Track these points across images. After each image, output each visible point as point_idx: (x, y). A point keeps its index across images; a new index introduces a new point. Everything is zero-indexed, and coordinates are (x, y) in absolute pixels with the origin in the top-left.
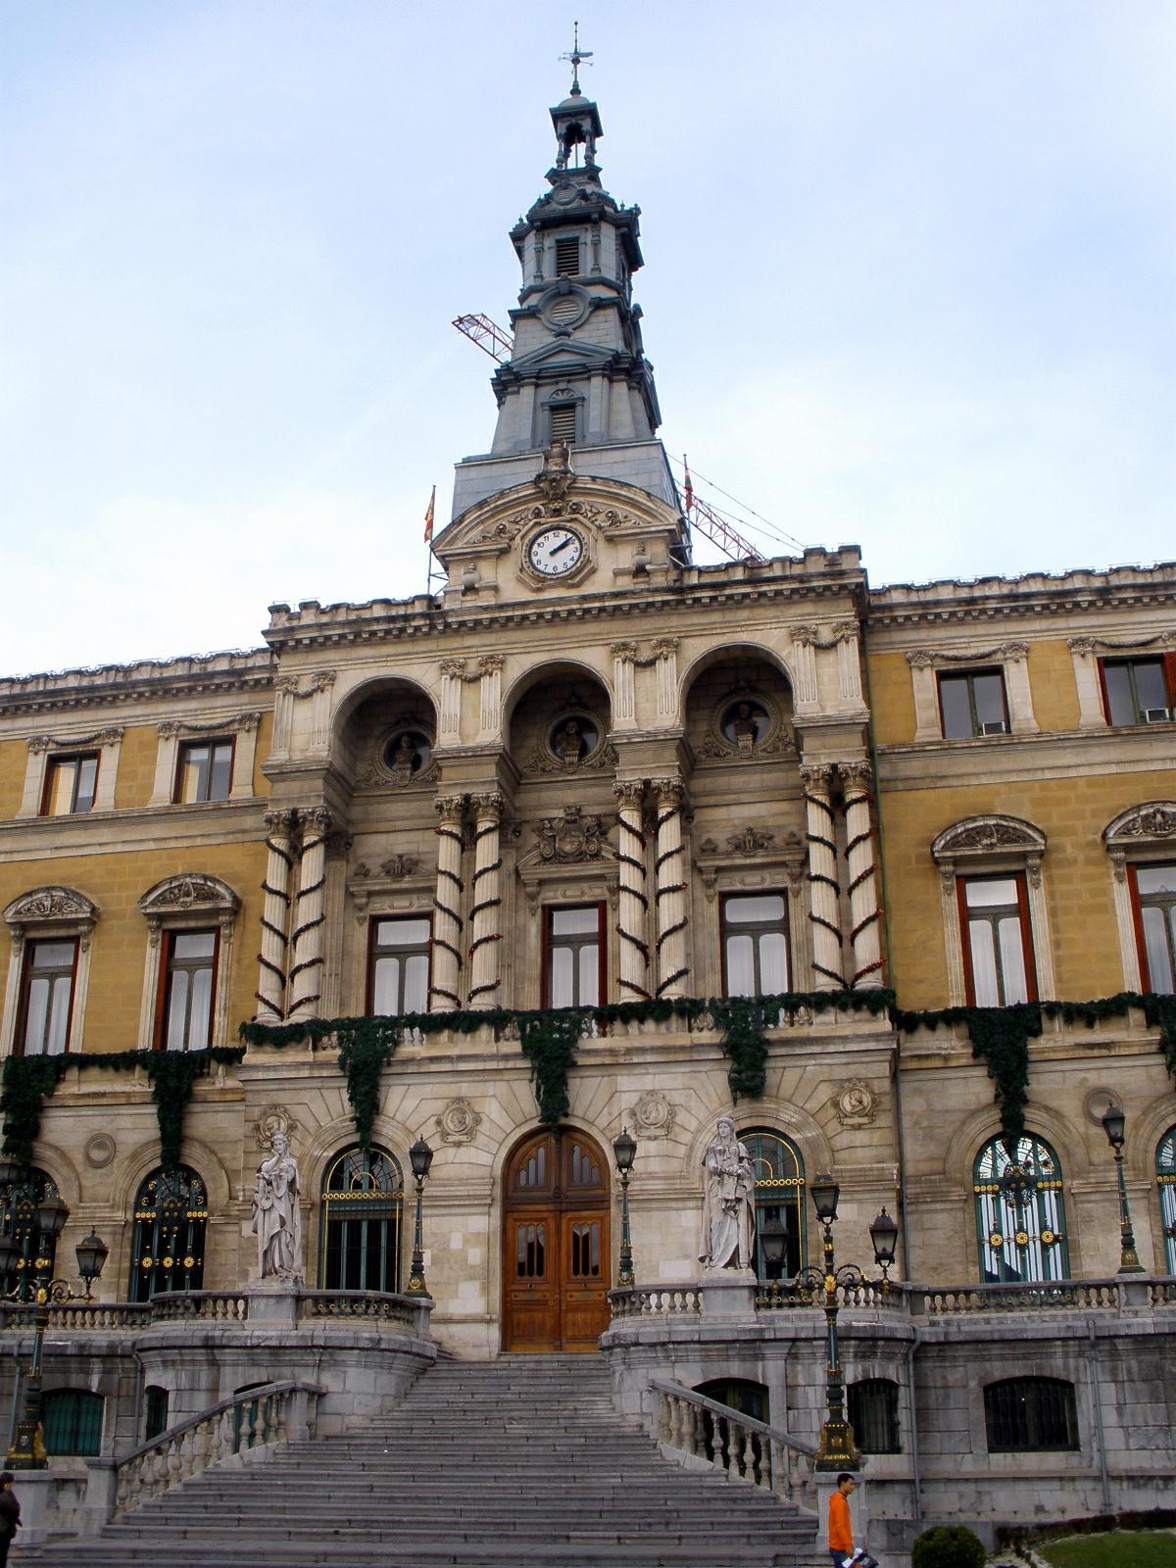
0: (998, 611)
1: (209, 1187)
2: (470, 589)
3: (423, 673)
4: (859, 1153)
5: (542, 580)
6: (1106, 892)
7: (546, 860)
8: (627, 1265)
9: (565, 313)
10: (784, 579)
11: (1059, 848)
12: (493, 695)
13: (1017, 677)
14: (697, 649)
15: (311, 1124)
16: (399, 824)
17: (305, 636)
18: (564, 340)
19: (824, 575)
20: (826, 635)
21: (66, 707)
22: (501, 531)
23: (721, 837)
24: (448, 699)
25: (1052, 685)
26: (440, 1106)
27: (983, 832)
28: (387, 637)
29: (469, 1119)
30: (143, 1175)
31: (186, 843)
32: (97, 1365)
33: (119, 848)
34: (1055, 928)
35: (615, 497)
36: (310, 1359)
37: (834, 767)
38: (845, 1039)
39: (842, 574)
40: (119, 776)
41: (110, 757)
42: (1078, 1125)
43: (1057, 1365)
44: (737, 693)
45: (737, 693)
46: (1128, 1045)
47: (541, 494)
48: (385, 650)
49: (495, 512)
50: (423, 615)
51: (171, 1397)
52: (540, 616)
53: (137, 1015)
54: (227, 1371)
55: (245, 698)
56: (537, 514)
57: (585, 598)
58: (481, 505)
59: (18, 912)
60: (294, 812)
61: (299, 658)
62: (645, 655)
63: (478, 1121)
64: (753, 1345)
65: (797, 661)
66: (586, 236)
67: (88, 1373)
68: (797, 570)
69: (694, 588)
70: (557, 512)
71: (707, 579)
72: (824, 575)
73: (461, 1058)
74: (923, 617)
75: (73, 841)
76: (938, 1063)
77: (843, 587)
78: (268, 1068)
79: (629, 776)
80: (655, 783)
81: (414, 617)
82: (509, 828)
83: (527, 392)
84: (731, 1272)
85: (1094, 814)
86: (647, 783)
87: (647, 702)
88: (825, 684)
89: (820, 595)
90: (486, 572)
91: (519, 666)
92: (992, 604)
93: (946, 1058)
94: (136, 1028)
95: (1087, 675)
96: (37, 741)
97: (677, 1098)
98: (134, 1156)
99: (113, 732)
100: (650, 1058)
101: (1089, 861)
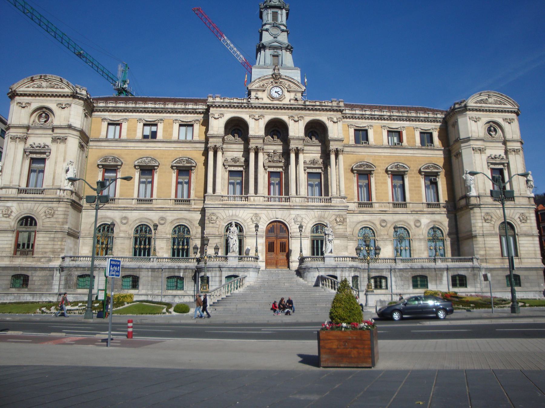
0: (368, 118)
1: (190, 230)
2: (257, 98)
4: (340, 230)
5: (273, 98)
6: (386, 180)
7: (270, 161)
8: (301, 251)
10: (328, 106)
11: (377, 170)
14: (308, 119)
15: (222, 218)
16: (235, 150)
17: (217, 104)
18: (275, 39)
19: (336, 106)
20: (335, 120)
21: (148, 112)
22: (263, 85)
23: (308, 161)
24: (252, 123)
26: (251, 215)
27: (364, 165)
28: (238, 107)
29: (258, 218)
30: (174, 227)
31: (182, 149)
32: (182, 271)
33: (164, 149)
34: (376, 186)
35: (290, 81)
36: (243, 270)
37: (337, 149)
38: (338, 206)
39: (340, 107)
40: (164, 131)
42: (379, 227)
43: (384, 274)
46: (389, 211)
47: (273, 78)
48: (237, 110)
49: (262, 80)
50: (246, 103)
51: (210, 278)
52: (273, 107)
53: (171, 189)
54: (223, 273)
55: (196, 115)
56: (272, 83)
57: (284, 104)
58: (259, 78)
59: (138, 162)
60: (215, 146)
61: (215, 109)
62: (296, 119)
63: (260, 219)
64: (335, 268)
65: (330, 125)
66: (279, 12)
67: (180, 272)
68: (330, 104)
69: (308, 105)
70: (276, 83)
71: (311, 104)
72: (336, 106)
73: (257, 205)
74: (352, 117)
75: (151, 146)
76: (352, 212)
77: (340, 110)
78: (212, 205)
80: (299, 148)
81: (244, 103)
83: (267, 51)
84: (330, 254)
85: (385, 163)
86: (297, 148)
87: (296, 130)
88: (335, 130)
89: (334, 111)
90: (260, 95)
91: (268, 118)
92: (367, 116)
93: (354, 211)
94: (171, 193)
95: (385, 133)
96: (140, 119)
97: (303, 216)
98: (171, 222)
99: (162, 120)
100: (298, 208)
101: (383, 173)
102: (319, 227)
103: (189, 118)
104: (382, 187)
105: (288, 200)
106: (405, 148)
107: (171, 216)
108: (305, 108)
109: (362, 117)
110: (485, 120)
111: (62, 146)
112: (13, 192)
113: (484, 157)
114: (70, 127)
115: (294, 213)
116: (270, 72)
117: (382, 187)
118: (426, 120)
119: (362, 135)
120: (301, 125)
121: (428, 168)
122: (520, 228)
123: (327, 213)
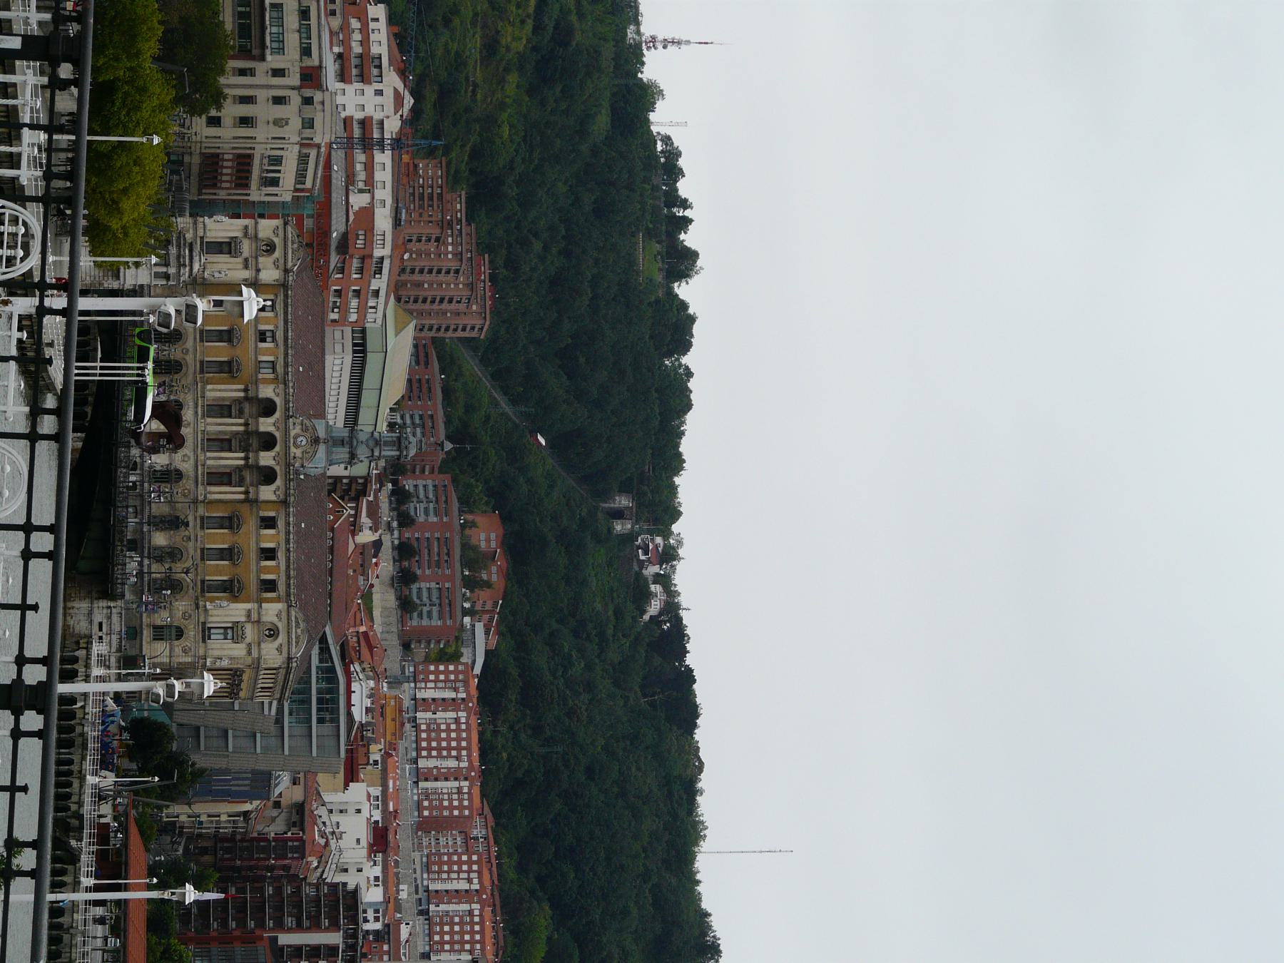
3: (277, 414)
5: (296, 437)
9: (371, 443)
12: (271, 429)
13: (272, 532)
14: (277, 468)
24: (271, 420)
25: (269, 538)
41: (271, 345)
44: (268, 476)
45: (268, 476)
64: (142, 469)
65: (273, 487)
79: (251, 455)
82: (246, 432)
87: (266, 459)
88: (267, 493)
91: (277, 434)
95: (271, 545)
102: (179, 475)
103: (280, 369)
104: (219, 539)
105: (202, 449)
106: (258, 563)
107: (189, 358)
108: (288, 465)
109: (288, 524)
110: (280, 625)
111: (241, 266)
112: (200, 233)
113: (243, 619)
114: (258, 271)
115: (191, 454)
116: (322, 433)
117: (219, 539)
118: (288, 586)
119: (269, 523)
120: (271, 463)
121: (239, 582)
122: (178, 646)
123: (191, 482)
